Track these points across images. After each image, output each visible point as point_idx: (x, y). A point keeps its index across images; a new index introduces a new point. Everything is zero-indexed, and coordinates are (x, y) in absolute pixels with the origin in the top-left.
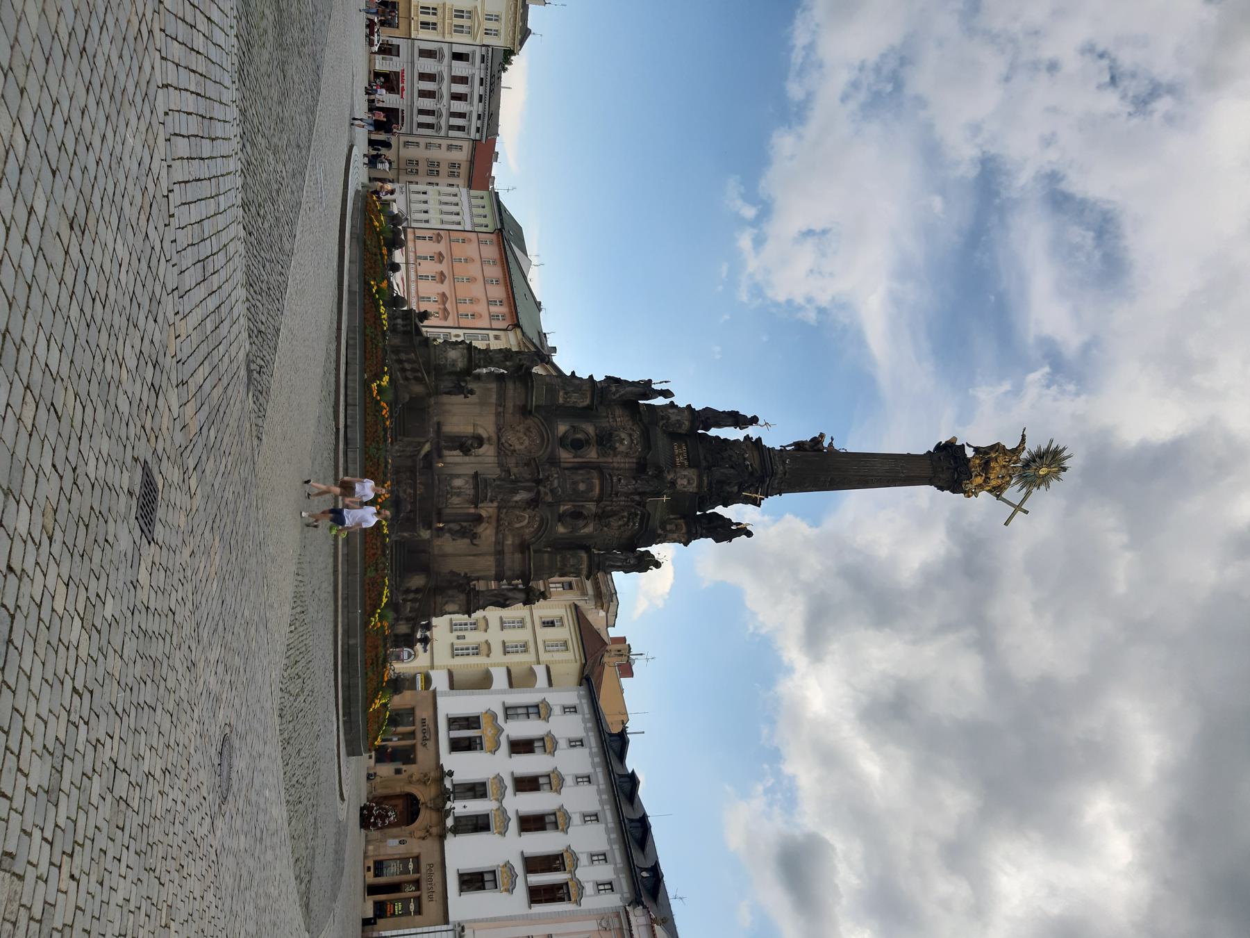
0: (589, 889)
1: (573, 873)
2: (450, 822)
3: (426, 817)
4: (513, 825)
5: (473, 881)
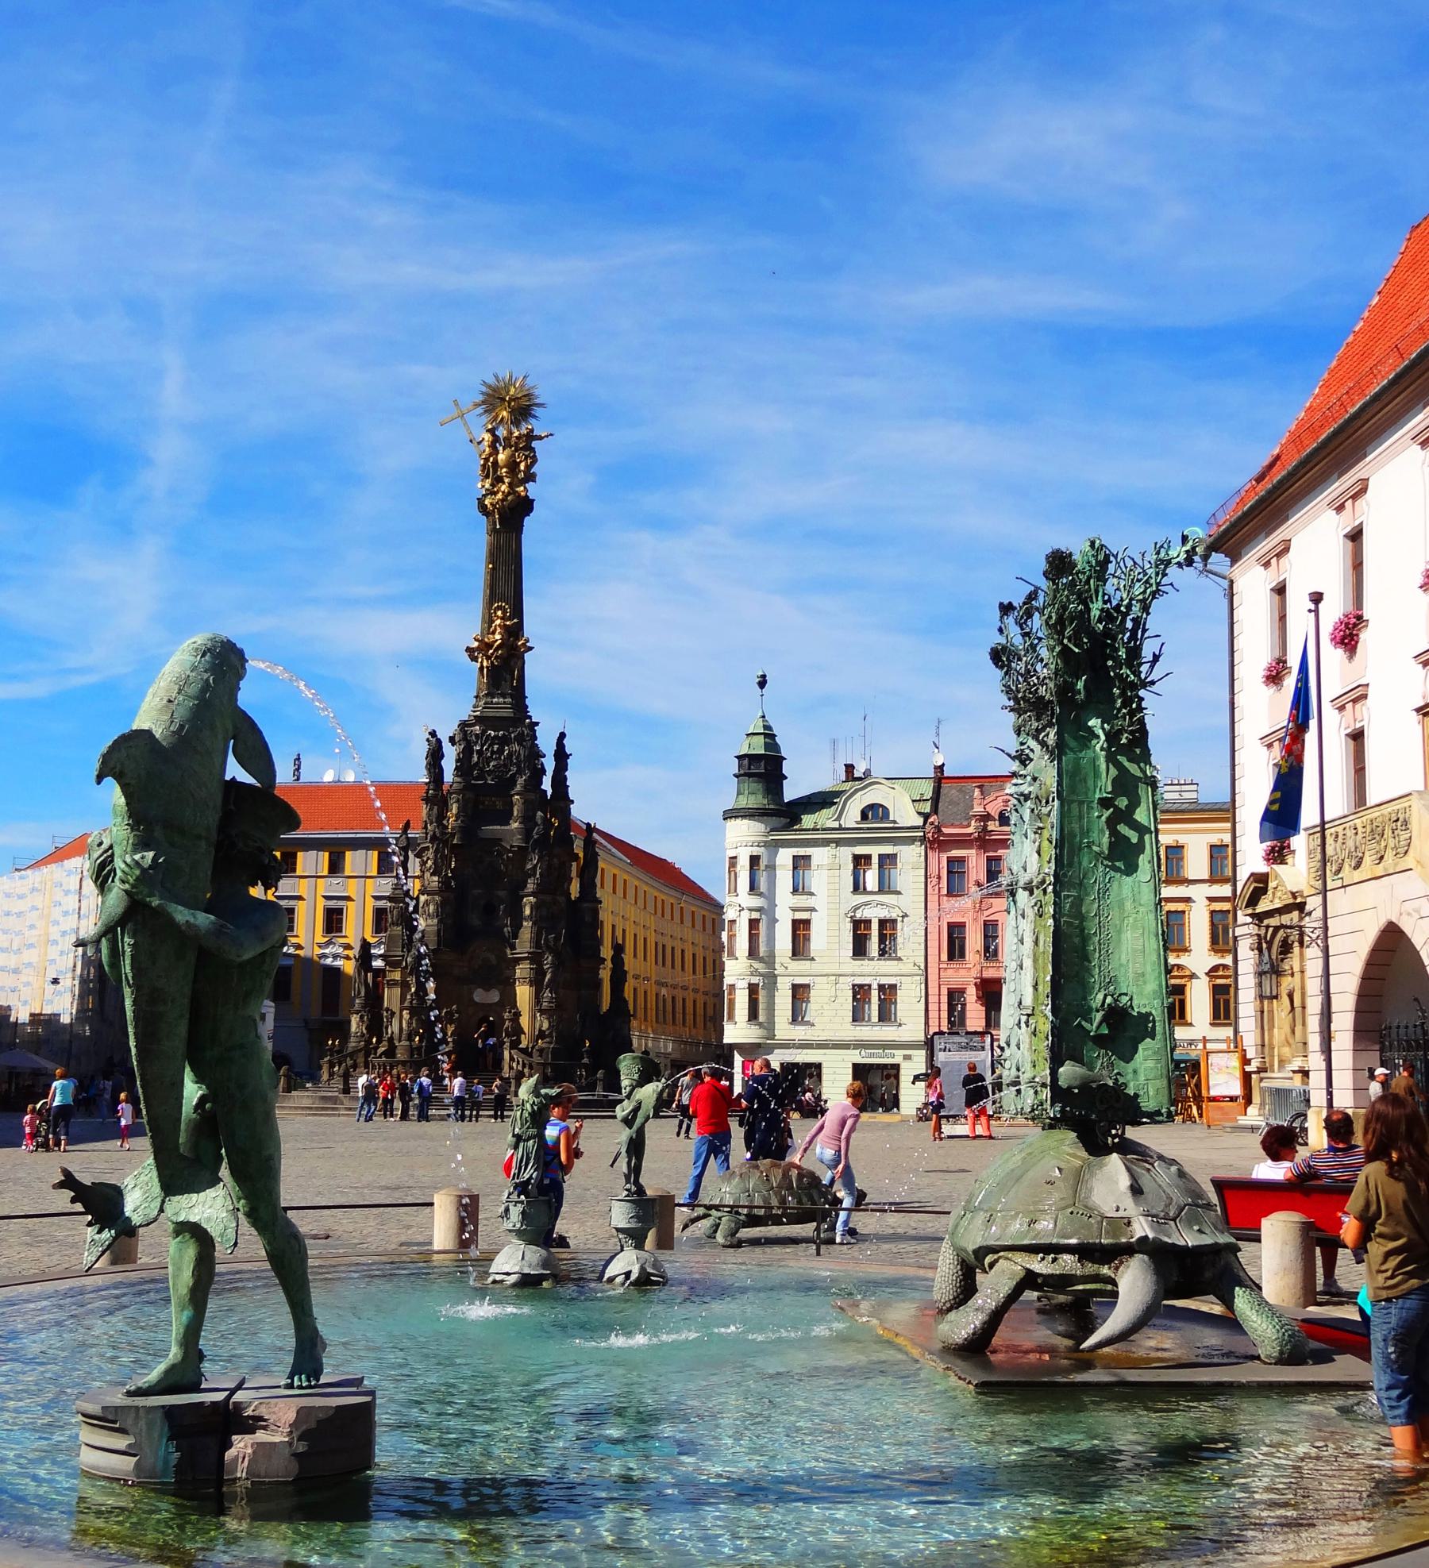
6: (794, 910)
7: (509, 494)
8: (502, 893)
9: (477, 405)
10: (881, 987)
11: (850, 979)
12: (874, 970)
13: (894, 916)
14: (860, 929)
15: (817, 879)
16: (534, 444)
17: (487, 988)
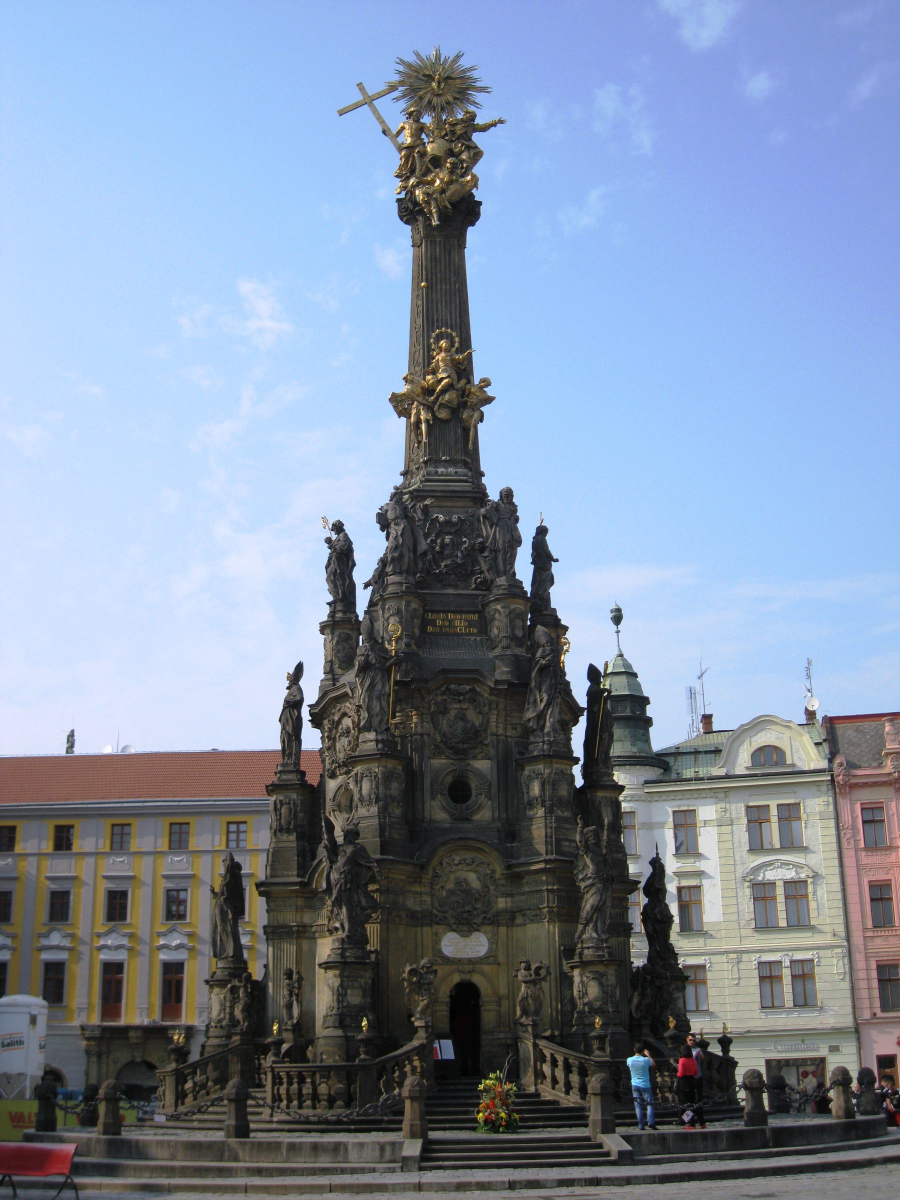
6: (679, 875)
7: (451, 182)
8: (483, 765)
9: (392, 88)
10: (792, 962)
11: (754, 957)
12: (784, 946)
13: (803, 876)
14: (762, 893)
15: (708, 840)
16: (477, 138)
17: (465, 925)
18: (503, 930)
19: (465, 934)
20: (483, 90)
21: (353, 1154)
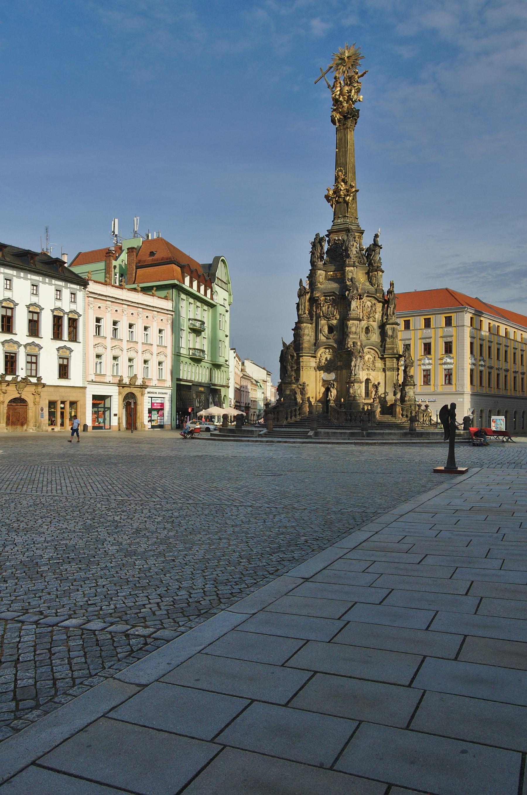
0: (73, 307)
1: (65, 313)
2: (34, 380)
3: (27, 394)
4: (36, 340)
5: (64, 371)
18: (339, 371)
19: (329, 373)
20: (363, 57)
21: (255, 433)
